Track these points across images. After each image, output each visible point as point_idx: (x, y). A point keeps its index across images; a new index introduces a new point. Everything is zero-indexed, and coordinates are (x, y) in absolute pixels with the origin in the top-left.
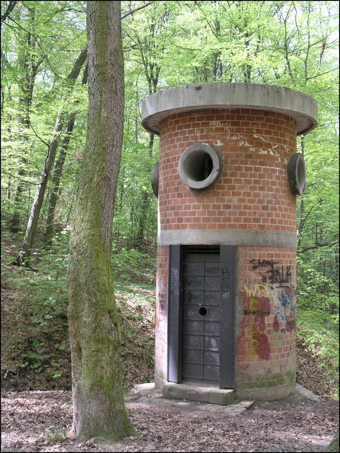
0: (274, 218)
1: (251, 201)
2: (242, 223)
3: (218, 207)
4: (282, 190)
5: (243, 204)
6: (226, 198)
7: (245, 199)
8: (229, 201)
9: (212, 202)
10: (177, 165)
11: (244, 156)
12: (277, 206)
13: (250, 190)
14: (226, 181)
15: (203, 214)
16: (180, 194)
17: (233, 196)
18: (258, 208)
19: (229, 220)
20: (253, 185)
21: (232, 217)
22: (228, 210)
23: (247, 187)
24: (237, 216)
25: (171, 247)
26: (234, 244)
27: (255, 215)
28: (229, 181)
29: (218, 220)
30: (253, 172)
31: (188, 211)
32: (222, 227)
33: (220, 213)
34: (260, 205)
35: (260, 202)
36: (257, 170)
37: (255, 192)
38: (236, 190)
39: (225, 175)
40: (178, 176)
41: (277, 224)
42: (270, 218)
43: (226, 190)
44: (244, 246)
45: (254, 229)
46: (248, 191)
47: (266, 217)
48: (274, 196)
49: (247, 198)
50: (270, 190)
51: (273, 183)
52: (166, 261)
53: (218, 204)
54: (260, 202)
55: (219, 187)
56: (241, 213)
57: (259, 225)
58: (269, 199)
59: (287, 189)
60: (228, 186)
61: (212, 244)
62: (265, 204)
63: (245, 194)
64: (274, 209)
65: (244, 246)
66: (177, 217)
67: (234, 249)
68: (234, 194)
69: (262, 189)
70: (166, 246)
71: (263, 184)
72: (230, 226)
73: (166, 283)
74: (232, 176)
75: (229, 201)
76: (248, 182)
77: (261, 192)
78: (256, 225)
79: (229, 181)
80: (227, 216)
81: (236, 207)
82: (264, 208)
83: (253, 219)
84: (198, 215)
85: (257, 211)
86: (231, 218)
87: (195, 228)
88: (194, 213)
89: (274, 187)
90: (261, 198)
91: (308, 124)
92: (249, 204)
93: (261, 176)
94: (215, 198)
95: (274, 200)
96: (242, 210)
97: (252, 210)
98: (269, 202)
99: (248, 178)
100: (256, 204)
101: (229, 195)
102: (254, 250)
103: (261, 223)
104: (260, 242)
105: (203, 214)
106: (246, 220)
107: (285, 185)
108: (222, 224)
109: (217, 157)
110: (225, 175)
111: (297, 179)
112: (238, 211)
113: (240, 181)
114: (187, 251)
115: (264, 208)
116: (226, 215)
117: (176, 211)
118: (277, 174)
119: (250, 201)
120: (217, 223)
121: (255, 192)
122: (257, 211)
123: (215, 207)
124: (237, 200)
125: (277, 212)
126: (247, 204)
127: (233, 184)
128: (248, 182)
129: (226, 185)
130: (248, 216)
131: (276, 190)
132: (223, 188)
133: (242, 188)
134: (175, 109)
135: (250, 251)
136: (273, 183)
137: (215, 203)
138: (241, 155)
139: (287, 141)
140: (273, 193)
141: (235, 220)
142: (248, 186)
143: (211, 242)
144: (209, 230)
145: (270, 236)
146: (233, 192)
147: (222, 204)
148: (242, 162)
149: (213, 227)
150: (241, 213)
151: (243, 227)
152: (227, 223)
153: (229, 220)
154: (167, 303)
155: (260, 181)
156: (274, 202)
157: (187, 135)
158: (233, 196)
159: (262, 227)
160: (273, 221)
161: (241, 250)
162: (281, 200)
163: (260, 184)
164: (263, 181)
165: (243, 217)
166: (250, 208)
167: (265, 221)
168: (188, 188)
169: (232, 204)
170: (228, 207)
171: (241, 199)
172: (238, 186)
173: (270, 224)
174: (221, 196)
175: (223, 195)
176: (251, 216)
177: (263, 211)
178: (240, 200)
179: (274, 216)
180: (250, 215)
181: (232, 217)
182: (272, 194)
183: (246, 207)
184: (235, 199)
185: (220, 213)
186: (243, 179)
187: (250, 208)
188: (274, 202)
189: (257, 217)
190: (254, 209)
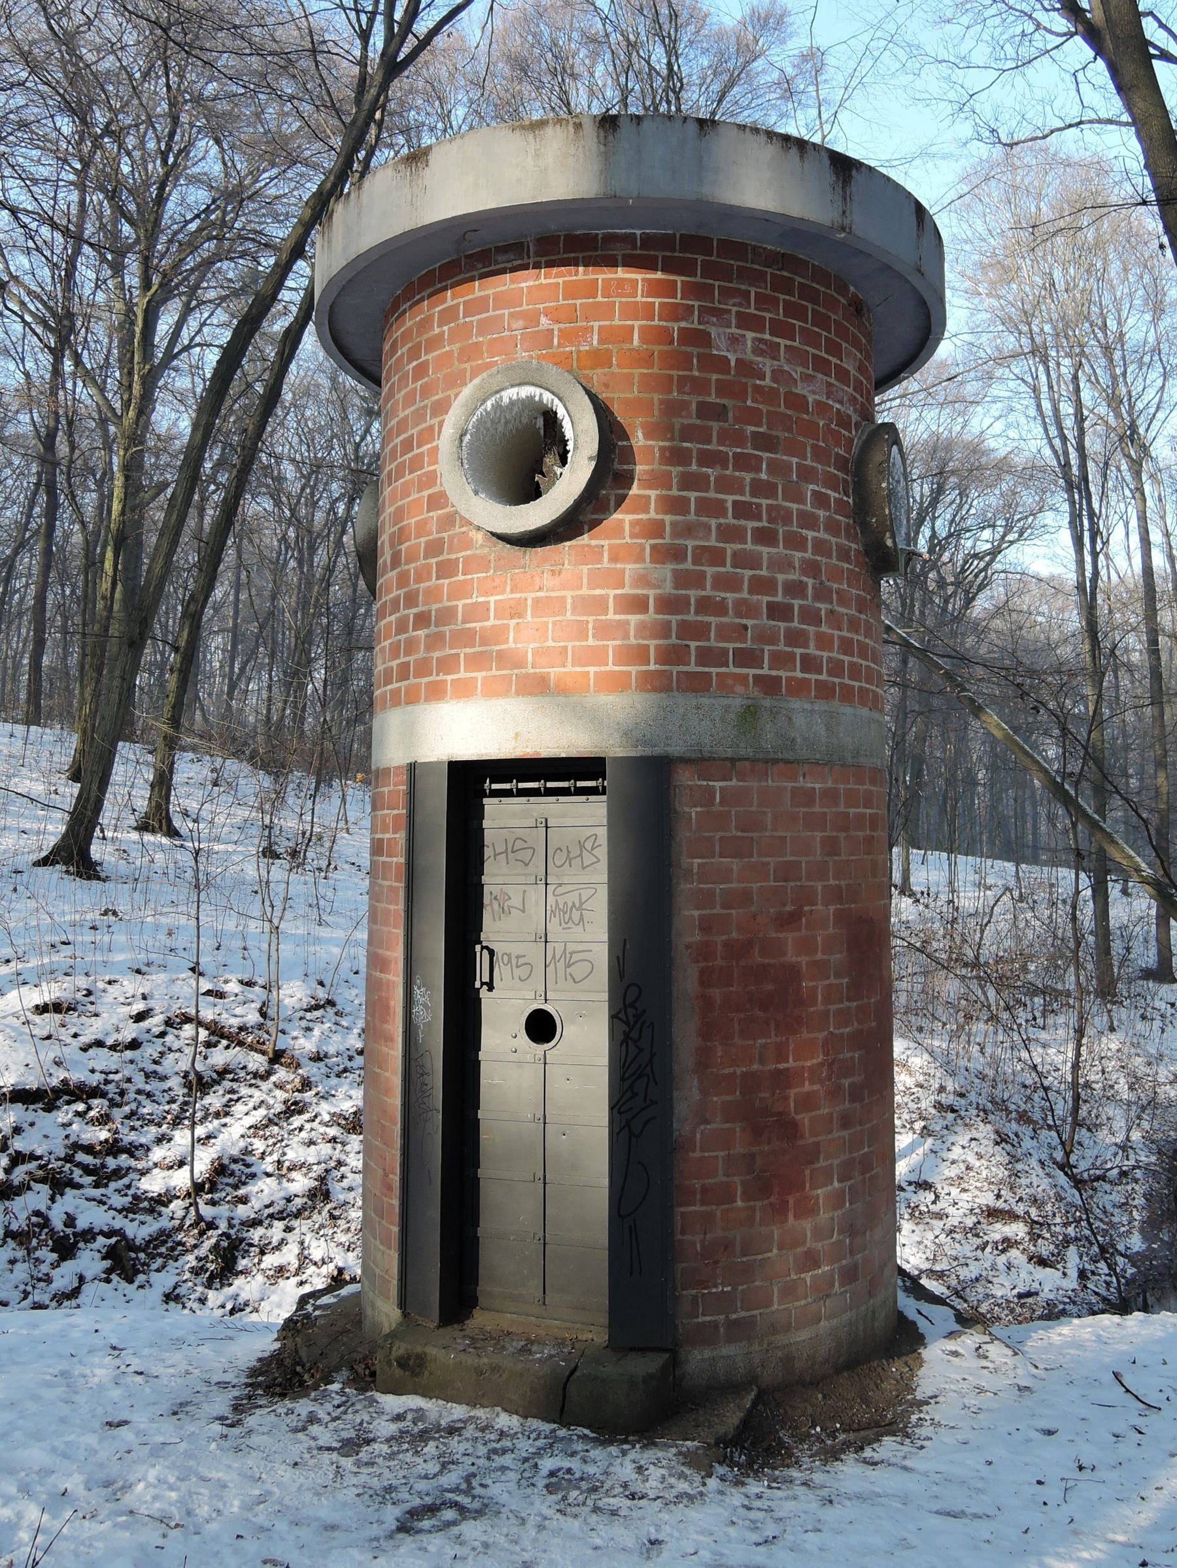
0: (812, 650)
2: (692, 668)
5: (693, 594)
7: (703, 575)
12: (823, 607)
35: (762, 585)
36: (744, 462)
40: (442, 495)
41: (824, 677)
44: (702, 762)
46: (713, 542)
48: (812, 569)
49: (710, 571)
50: (796, 542)
51: (808, 521)
54: (762, 585)
58: (794, 576)
69: (765, 537)
82: (778, 612)
89: (810, 534)
98: (795, 589)
99: (712, 495)
100: (745, 594)
102: (742, 777)
106: (706, 656)
115: (778, 612)
125: (824, 628)
130: (713, 643)
140: (808, 555)
142: (713, 523)
145: (799, 720)
159: (770, 685)
160: (809, 664)
161: (686, 778)
165: (693, 644)
166: (720, 609)
168: (479, 537)
173: (798, 674)
179: (812, 644)
183: (704, 605)
187: (720, 609)
189: (748, 644)
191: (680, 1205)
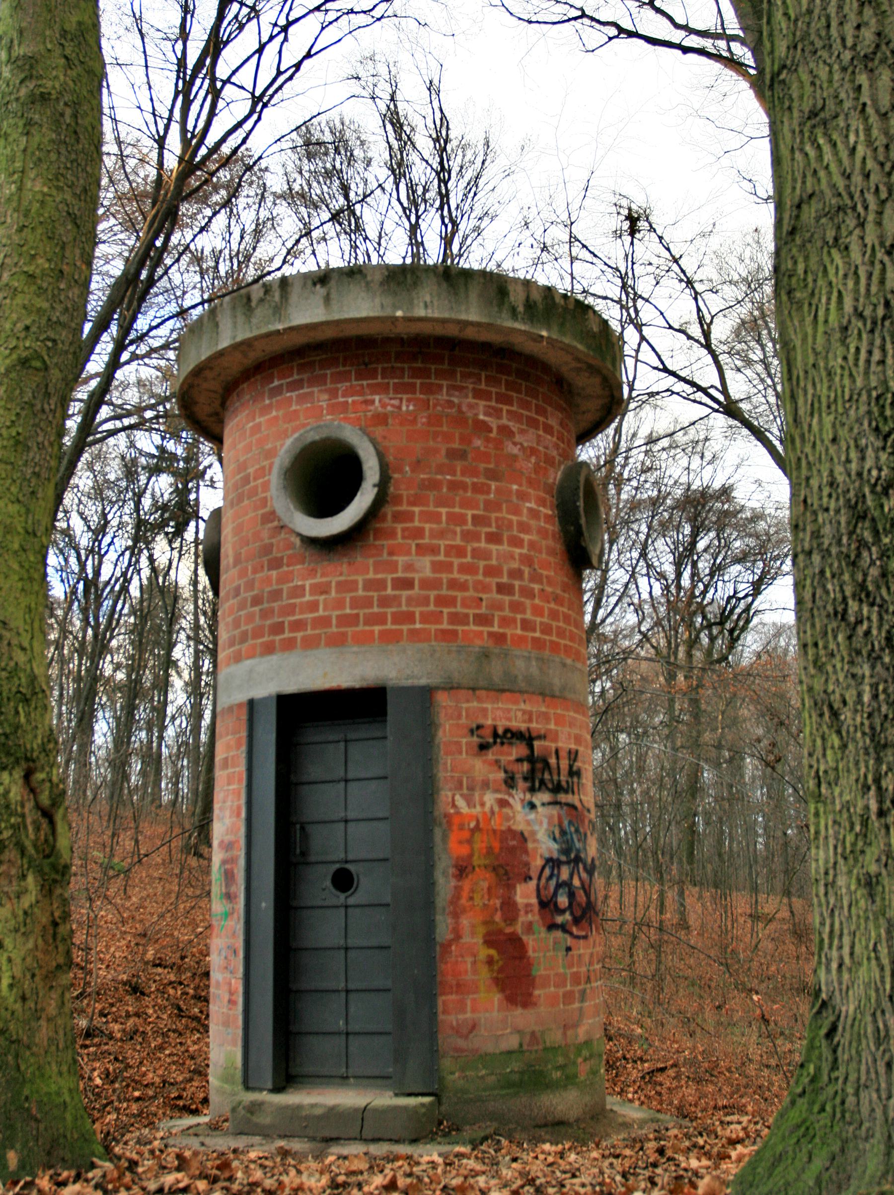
0: (528, 616)
1: (466, 569)
2: (445, 626)
3: (379, 585)
4: (548, 547)
5: (444, 576)
6: (401, 560)
7: (451, 564)
8: (409, 567)
9: (359, 571)
10: (266, 486)
11: (443, 452)
12: (536, 587)
13: (462, 539)
14: (398, 517)
15: (340, 604)
16: (276, 559)
17: (417, 554)
18: (485, 588)
19: (409, 617)
20: (470, 526)
21: (418, 610)
22: (405, 593)
23: (455, 533)
24: (432, 607)
25: (251, 703)
26: (423, 682)
27: (479, 606)
28: (409, 517)
29: (380, 619)
30: (469, 494)
31: (298, 601)
32: (390, 637)
33: (384, 602)
34: (493, 581)
35: (491, 571)
36: (479, 489)
37: (476, 545)
38: (426, 541)
39: (398, 500)
40: (273, 513)
41: (537, 635)
42: (519, 616)
43: (400, 540)
44: (451, 687)
45: (478, 642)
46: (458, 541)
47: (507, 613)
48: (527, 560)
49: (456, 561)
50: (516, 542)
51: (524, 527)
52: (238, 746)
53: (380, 576)
54: (491, 571)
55: (378, 534)
56: (442, 601)
57: (490, 634)
58: (515, 565)
59: (559, 547)
60: (404, 530)
61: (364, 684)
62: (505, 579)
63: (449, 550)
64: (527, 593)
65: (452, 688)
66: (268, 622)
67: (424, 696)
68: (422, 550)
69: (494, 538)
70: (240, 705)
71: (498, 527)
72: (414, 635)
73: (239, 808)
74: (414, 504)
75: (409, 567)
76: (458, 519)
77: (494, 547)
78: (481, 633)
79: (409, 517)
80: (404, 608)
81: (426, 584)
82: (502, 589)
83: (475, 615)
84: (325, 610)
85: (484, 596)
86: (413, 613)
87: (318, 646)
88: (313, 606)
89: (526, 537)
90: (494, 562)
91: (601, 402)
92: (463, 577)
93: (489, 506)
94: (371, 561)
95: (526, 570)
96: (444, 592)
97: (471, 593)
98: (516, 574)
99: (457, 510)
100: (480, 577)
101: (408, 553)
102: (479, 700)
103: (496, 629)
104: (496, 679)
105: (340, 604)
106: (455, 619)
107: (554, 536)
108: (391, 631)
109: (371, 449)
110: (398, 500)
111: (583, 521)
112: (432, 594)
113: (435, 517)
114: (300, 717)
115: (502, 589)
116: (400, 605)
117: (265, 605)
118: (533, 519)
119: (464, 569)
120: (377, 628)
121: (476, 545)
122: (484, 596)
123: (370, 585)
124: (428, 565)
125: (537, 601)
126: (456, 575)
127: (417, 524)
128: (458, 519)
129: (399, 527)
130: (459, 609)
131: (532, 545)
132: (392, 534)
133: (441, 534)
134: (256, 338)
135: (468, 701)
136: (524, 527)
137: (371, 575)
138: (436, 451)
139: (552, 427)
140: (525, 551)
141: (425, 618)
142: (458, 529)
143: (363, 679)
144: (355, 649)
145: (520, 664)
146: (417, 545)
147: (389, 577)
148: (440, 469)
149: (364, 639)
150: (442, 601)
151: (448, 636)
152: (405, 628)
153: (409, 617)
154: (242, 862)
155: (489, 518)
156: (526, 575)
157: (294, 408)
158: (417, 554)
159: (500, 638)
160: (527, 625)
161: (443, 699)
162: (545, 573)
163: (490, 526)
164: (497, 519)
165: (446, 611)
166: (463, 587)
167: (505, 622)
168: (297, 541)
169: (417, 576)
170: (407, 584)
171: (441, 562)
172: (431, 530)
173: (519, 632)
174: (385, 556)
175: (391, 553)
176: (469, 607)
177: (499, 597)
178: (438, 567)
179: (529, 611)
180: (464, 605)
181: (418, 610)
182: (521, 555)
183: (453, 584)
184: (425, 564)
185: (384, 602)
186: (444, 510)
187: (463, 587)
188: (526, 575)
189: (483, 610)
190: (476, 590)
191: (444, 994)
